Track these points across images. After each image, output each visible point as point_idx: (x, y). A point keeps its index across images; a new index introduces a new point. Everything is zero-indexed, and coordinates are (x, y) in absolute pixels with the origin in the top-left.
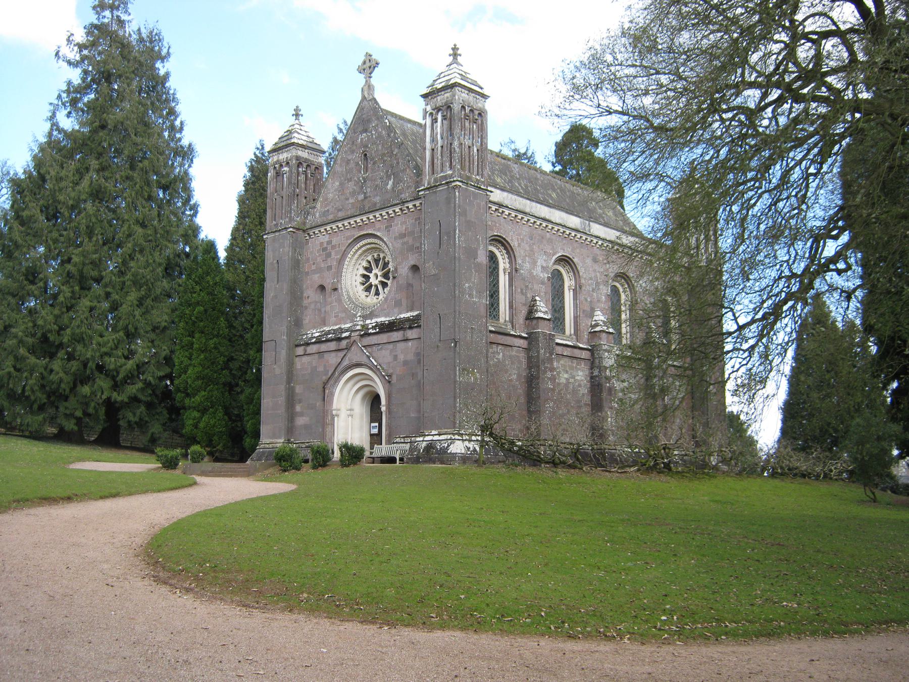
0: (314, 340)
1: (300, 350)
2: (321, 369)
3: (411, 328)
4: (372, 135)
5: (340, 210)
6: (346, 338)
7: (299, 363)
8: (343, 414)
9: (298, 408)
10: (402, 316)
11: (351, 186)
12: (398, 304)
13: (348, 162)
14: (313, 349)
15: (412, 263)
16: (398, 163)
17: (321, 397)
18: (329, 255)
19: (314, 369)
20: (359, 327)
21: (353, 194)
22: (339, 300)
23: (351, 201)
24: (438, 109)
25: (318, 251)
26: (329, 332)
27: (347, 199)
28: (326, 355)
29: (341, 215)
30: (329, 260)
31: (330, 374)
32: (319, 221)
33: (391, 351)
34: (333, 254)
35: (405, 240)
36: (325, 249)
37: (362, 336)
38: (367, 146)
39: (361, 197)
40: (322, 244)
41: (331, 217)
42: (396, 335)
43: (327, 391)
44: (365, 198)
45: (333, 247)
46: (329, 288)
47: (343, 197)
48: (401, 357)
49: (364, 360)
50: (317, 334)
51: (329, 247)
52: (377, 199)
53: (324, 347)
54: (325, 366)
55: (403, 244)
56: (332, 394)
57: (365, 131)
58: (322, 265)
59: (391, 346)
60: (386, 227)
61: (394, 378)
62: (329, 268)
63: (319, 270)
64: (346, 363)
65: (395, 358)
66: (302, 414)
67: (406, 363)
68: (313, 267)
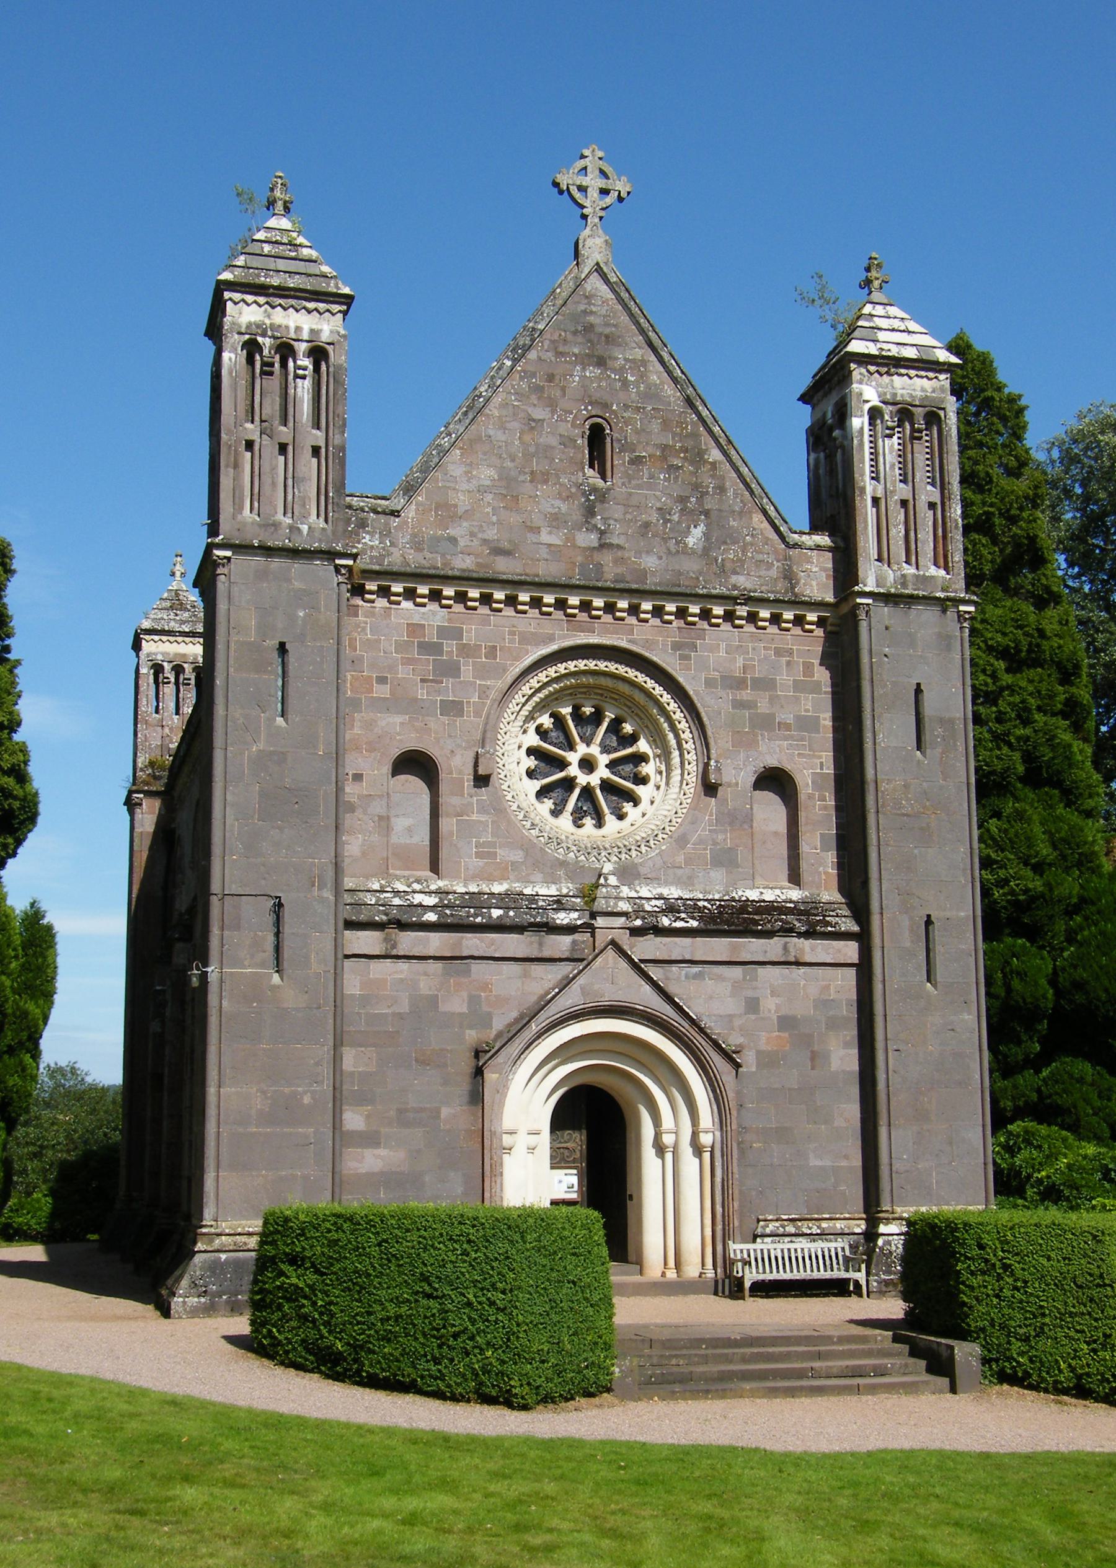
0: (431, 917)
1: (366, 941)
2: (457, 1004)
3: (809, 934)
4: (625, 383)
5: (507, 553)
6: (570, 929)
7: (354, 980)
8: (521, 1142)
9: (354, 1120)
10: (753, 895)
11: (547, 501)
12: (724, 859)
13: (532, 424)
14: (408, 941)
15: (772, 762)
16: (721, 489)
17: (463, 1086)
18: (453, 670)
19: (426, 1008)
20: (624, 906)
21: (555, 520)
22: (498, 808)
23: (546, 537)
24: (904, 413)
25: (401, 647)
26: (475, 900)
27: (537, 530)
28: (476, 967)
29: (505, 567)
30: (448, 682)
31: (499, 1023)
32: (415, 560)
33: (737, 987)
34: (467, 671)
35: (746, 694)
36: (428, 648)
37: (635, 932)
38: (606, 406)
39: (593, 539)
40: (415, 629)
41: (463, 563)
42: (753, 947)
43: (490, 1076)
44: (602, 546)
45: (466, 651)
46: (455, 766)
47: (514, 519)
48: (770, 1005)
49: (645, 997)
50: (431, 901)
51: (450, 646)
52: (650, 562)
53: (472, 943)
54: (474, 1001)
55: (739, 704)
56: (502, 1089)
57: (601, 362)
58: (422, 693)
59: (738, 971)
60: (676, 646)
61: (749, 1060)
62: (453, 708)
63: (411, 706)
64: (571, 999)
65: (753, 1005)
66: (370, 1139)
67: (786, 1022)
68: (382, 691)
